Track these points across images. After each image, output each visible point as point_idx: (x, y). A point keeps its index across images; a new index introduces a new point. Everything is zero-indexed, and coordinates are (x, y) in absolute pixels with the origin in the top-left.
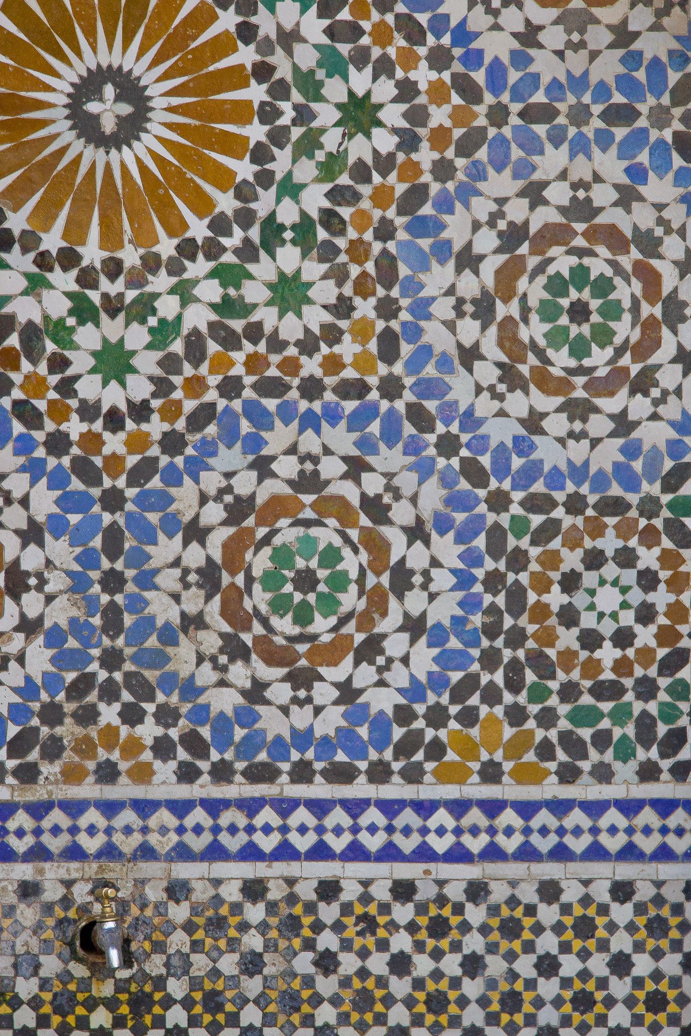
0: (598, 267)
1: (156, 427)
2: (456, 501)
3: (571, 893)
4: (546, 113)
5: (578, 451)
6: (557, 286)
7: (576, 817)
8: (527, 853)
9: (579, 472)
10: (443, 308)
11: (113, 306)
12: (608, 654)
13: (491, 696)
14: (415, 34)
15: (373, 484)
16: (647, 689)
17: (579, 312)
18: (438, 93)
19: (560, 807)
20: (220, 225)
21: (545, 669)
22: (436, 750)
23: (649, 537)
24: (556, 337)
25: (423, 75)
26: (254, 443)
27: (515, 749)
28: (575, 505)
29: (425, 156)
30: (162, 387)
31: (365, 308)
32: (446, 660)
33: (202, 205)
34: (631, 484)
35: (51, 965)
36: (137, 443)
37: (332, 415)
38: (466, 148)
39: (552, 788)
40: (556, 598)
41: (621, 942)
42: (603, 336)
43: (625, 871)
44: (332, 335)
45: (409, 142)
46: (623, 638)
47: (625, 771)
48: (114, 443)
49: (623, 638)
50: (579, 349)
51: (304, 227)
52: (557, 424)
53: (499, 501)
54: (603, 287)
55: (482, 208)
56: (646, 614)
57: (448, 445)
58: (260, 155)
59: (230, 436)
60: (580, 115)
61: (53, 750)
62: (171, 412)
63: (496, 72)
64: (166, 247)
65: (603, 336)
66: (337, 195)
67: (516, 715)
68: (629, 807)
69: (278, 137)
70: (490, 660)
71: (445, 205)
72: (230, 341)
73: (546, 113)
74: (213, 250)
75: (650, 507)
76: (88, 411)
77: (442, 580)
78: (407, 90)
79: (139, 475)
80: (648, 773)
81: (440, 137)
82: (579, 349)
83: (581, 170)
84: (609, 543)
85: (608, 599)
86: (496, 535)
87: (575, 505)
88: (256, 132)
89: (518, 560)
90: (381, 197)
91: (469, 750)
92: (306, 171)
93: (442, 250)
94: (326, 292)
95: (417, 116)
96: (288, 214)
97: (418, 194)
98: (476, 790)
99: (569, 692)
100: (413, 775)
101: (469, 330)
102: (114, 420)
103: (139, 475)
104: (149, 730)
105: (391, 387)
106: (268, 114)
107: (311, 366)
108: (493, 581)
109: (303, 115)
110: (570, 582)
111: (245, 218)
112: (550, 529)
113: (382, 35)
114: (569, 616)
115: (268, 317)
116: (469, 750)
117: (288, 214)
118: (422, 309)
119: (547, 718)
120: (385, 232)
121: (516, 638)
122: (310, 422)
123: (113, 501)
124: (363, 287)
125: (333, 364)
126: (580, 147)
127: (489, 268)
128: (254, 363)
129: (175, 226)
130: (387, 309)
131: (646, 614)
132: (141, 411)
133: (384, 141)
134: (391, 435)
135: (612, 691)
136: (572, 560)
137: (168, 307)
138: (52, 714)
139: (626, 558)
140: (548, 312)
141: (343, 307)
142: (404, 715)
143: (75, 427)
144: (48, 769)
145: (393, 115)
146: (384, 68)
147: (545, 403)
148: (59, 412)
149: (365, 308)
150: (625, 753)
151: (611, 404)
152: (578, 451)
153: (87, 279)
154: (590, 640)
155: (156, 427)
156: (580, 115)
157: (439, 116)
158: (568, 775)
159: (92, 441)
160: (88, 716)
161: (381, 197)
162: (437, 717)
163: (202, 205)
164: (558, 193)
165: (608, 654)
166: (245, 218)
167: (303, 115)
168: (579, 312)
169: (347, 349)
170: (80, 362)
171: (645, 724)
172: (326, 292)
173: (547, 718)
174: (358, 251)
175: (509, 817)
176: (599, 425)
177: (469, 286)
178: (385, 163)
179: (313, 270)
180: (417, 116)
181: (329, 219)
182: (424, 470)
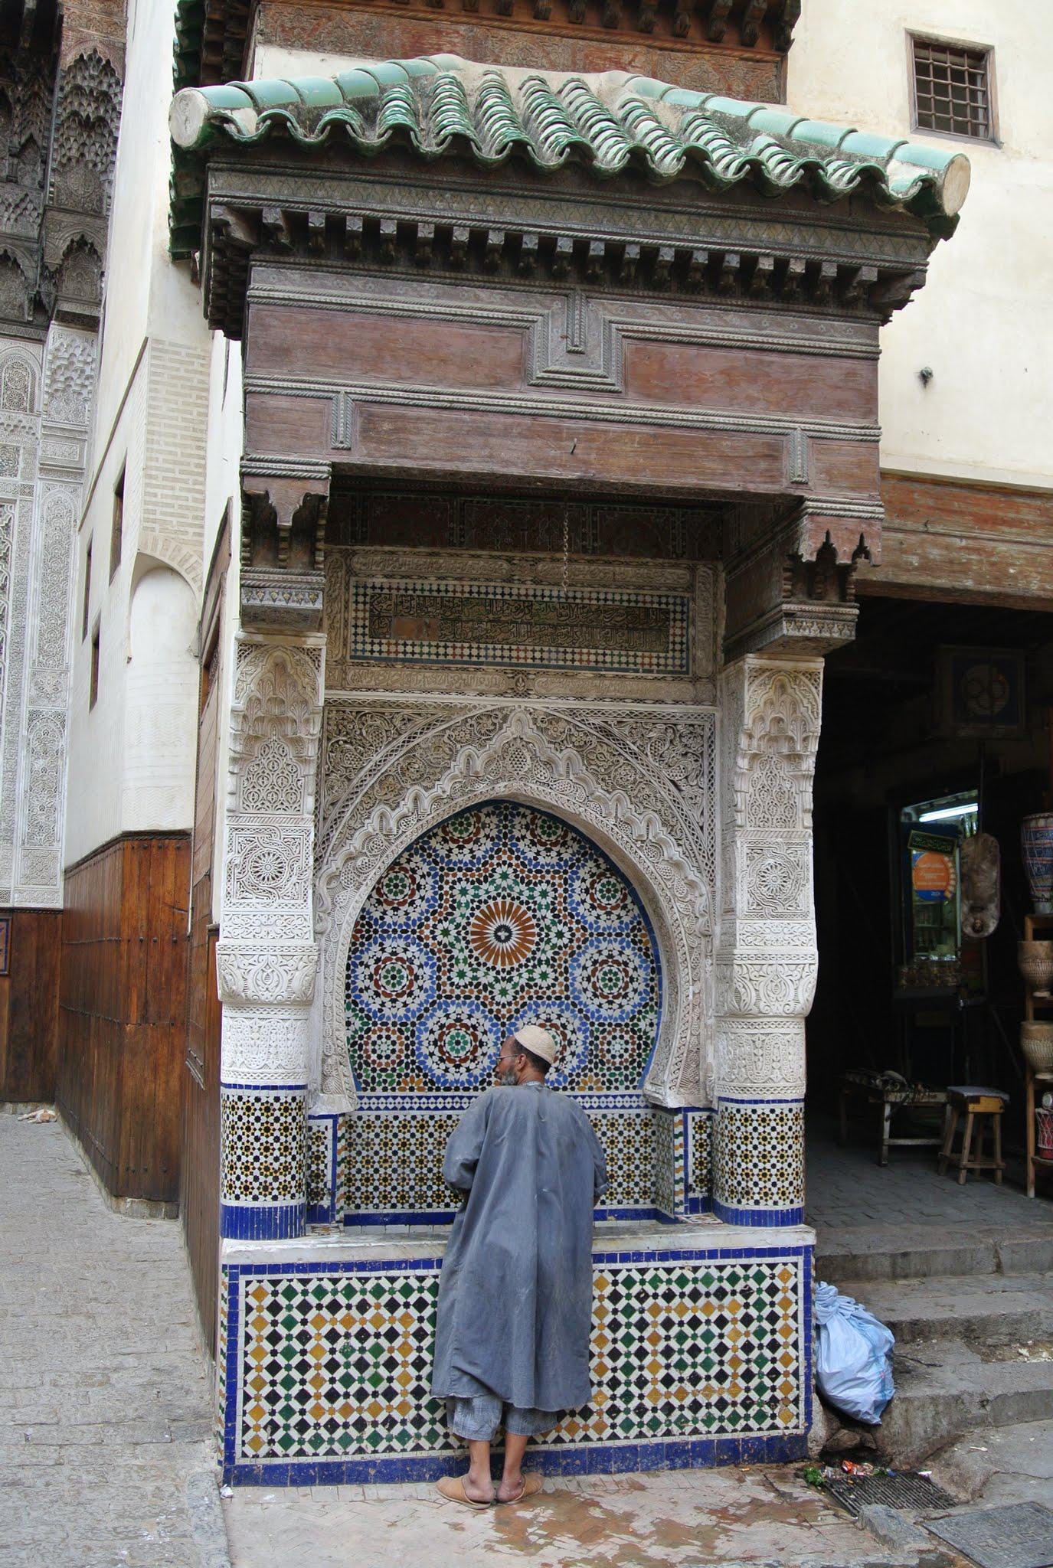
0: (614, 969)
1: (513, 1007)
2: (584, 1024)
3: (609, 1117)
4: (601, 934)
5: (610, 1012)
6: (605, 974)
7: (611, 1099)
8: (599, 1107)
9: (611, 1017)
10: (579, 979)
11: (504, 979)
12: (618, 1060)
13: (591, 1070)
14: (572, 917)
15: (563, 1020)
16: (626, 1068)
17: (610, 980)
18: (578, 930)
19: (607, 1096)
20: (528, 960)
21: (603, 1064)
22: (578, 1083)
23: (627, 1032)
24: (605, 986)
25: (574, 926)
26: (536, 1011)
27: (597, 1082)
28: (610, 1025)
29: (575, 944)
30: (515, 998)
31: (561, 979)
32: (581, 1061)
33: (524, 956)
34: (622, 1019)
36: (509, 1011)
37: (554, 1004)
38: (584, 942)
39: (605, 1092)
40: (606, 1047)
41: (621, 1128)
42: (616, 985)
43: (622, 1111)
44: (554, 985)
45: (571, 941)
46: (621, 1056)
47: (622, 1088)
48: (504, 1011)
49: (621, 1056)
50: (611, 988)
51: (547, 962)
52: (606, 1006)
53: (592, 1024)
54: (616, 974)
55: (588, 956)
56: (626, 1050)
57: (580, 1011)
58: (538, 944)
59: (530, 1009)
60: (610, 935)
61: (489, 1083)
62: (517, 1004)
63: (591, 925)
64: (516, 965)
65: (616, 985)
66: (556, 953)
67: (596, 1075)
68: (623, 1096)
69: (542, 940)
70: (591, 1062)
71: (579, 955)
72: (530, 987)
73: (601, 934)
74: (526, 966)
75: (627, 1025)
76: (498, 1004)
77: (579, 1043)
78: (571, 929)
79: (510, 1018)
80: (627, 1088)
81: (578, 940)
82: (611, 988)
83: (610, 947)
84: (618, 1034)
85: (618, 1047)
86: (592, 1032)
87: (610, 1025)
88: (536, 939)
89: (597, 1038)
90: (565, 953)
91: (585, 1083)
92: (548, 947)
93: (579, 966)
94: (552, 975)
95: (573, 935)
96: (544, 958)
97: (572, 954)
98: (587, 1092)
99: (609, 1069)
100: (573, 1089)
101: (585, 984)
102: (504, 1006)
103: (510, 1018)
105: (567, 998)
106: (539, 935)
107: (549, 993)
108: (591, 1043)
109: (547, 935)
110: (609, 1043)
111: (534, 958)
112: (604, 1031)
113: (565, 917)
114: (609, 1051)
115: (539, 981)
116: (585, 1083)
117: (544, 958)
118: (574, 979)
119: (604, 1075)
120: (566, 961)
121: (596, 1056)
122: (549, 1006)
123: (503, 1024)
124: (561, 974)
125: (554, 992)
126: (610, 942)
127: (590, 969)
128: (536, 992)
129: (518, 960)
130: (566, 979)
131: (626, 1050)
132: (510, 1004)
133: (566, 941)
134: (567, 1009)
136: (609, 1038)
137: (516, 979)
139: (622, 1037)
140: (603, 980)
141: (556, 979)
142: (571, 1075)
143: (495, 1007)
145: (568, 935)
146: (565, 924)
147: (603, 1001)
148: (491, 1004)
149: (561, 979)
150: (622, 1083)
151: (617, 1001)
152: (610, 1012)
153: (498, 973)
154: (614, 1057)
155: (513, 1007)
156: (610, 935)
157: (578, 935)
158: (609, 1088)
159: (499, 1011)
161: (565, 953)
162: (578, 1075)
163: (524, 956)
164: (605, 953)
165: (618, 1060)
166: (534, 958)
167: (547, 935)
168: (610, 980)
169: (557, 988)
170: (496, 992)
171: (626, 1077)
172: (552, 975)
173: (604, 1075)
174: (560, 966)
175: (595, 1099)
176: (615, 1006)
177: (585, 974)
178: (566, 946)
179: (549, 970)
180: (573, 935)
182: (575, 1017)
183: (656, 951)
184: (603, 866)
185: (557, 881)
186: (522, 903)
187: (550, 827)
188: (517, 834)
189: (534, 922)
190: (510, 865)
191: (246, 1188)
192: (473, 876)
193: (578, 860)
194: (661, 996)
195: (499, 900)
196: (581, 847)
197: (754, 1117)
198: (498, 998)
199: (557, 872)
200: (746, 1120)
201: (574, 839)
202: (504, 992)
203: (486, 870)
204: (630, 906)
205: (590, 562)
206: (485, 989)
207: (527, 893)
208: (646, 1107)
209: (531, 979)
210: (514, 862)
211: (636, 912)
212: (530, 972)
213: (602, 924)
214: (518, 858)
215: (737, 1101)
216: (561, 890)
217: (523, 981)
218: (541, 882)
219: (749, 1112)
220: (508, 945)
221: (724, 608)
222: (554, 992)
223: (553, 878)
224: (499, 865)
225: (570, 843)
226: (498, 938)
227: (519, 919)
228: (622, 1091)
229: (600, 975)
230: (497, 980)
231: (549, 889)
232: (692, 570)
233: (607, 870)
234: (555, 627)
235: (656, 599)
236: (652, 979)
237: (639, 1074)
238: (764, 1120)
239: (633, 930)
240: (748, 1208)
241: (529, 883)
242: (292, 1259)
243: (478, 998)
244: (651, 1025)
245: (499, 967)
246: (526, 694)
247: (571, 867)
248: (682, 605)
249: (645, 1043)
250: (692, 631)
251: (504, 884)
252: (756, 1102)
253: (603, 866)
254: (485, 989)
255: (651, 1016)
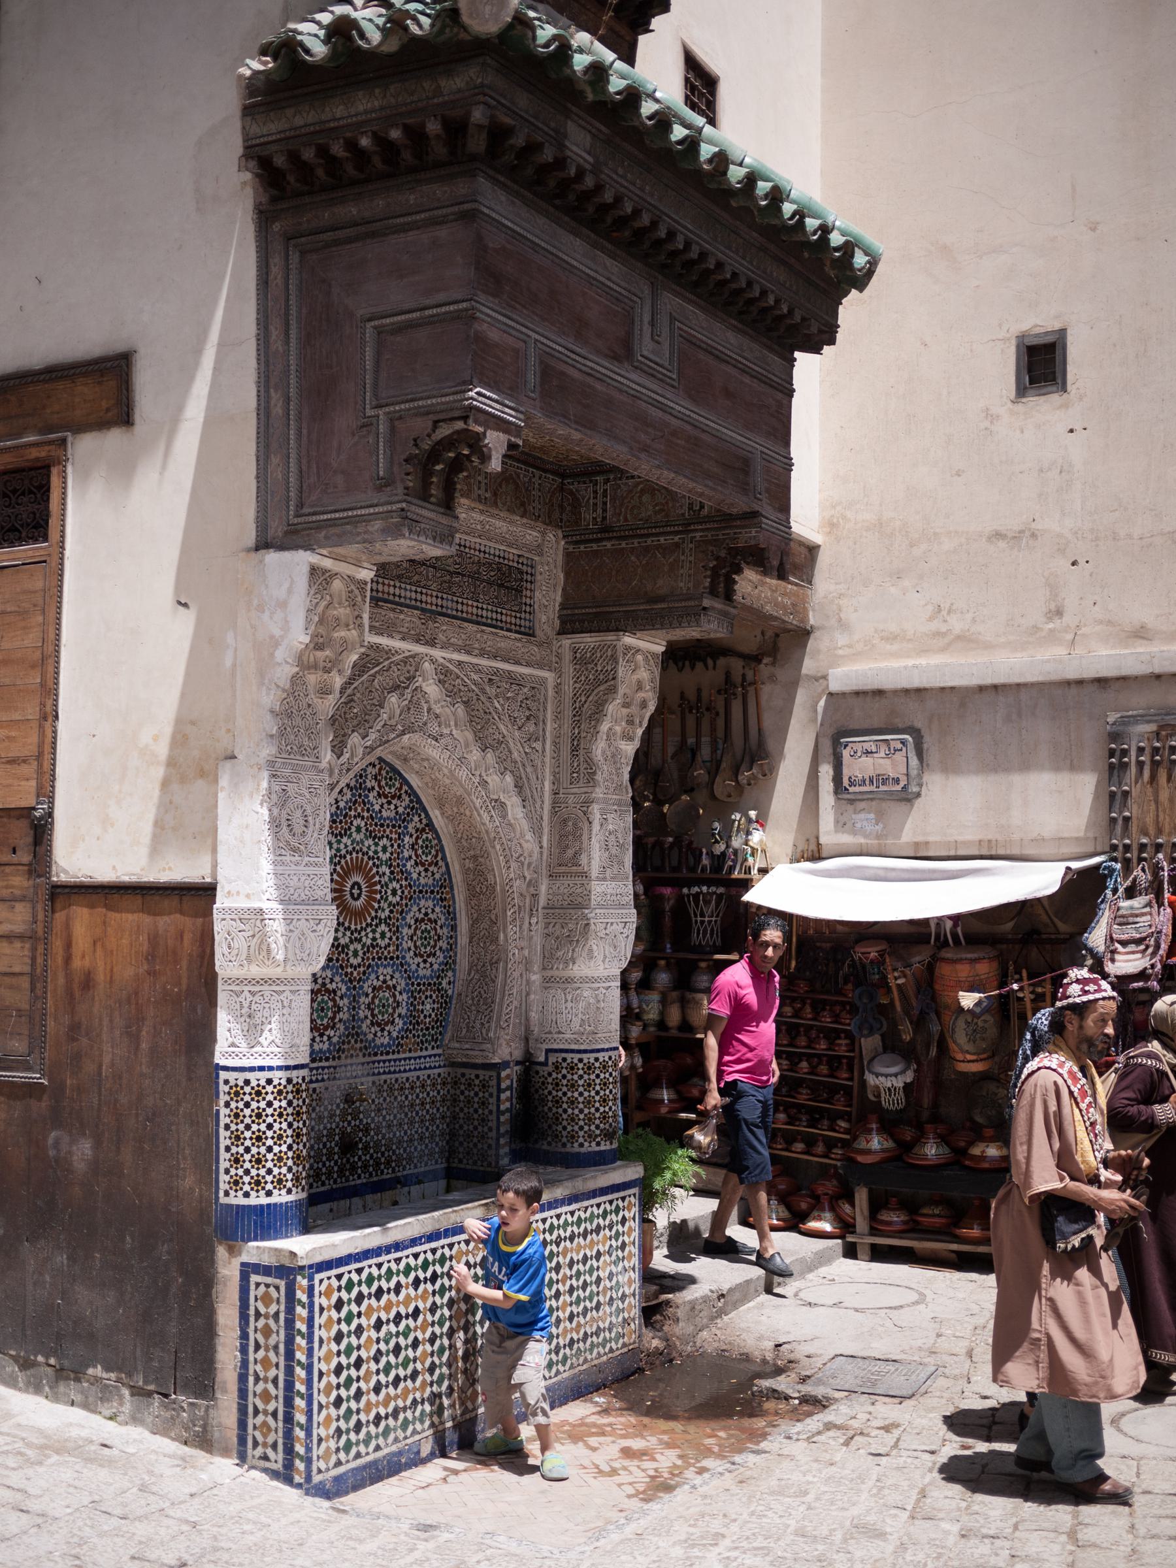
1: (362, 969)
35: (342, 1106)
44: (389, 945)
53: (413, 984)
57: (406, 971)
66: (391, 912)
76: (351, 966)
80: (433, 1048)
84: (428, 993)
91: (407, 1045)
95: (403, 892)
104: (358, 1045)
105: (398, 958)
110: (423, 1003)
115: (379, 941)
123: (354, 988)
130: (397, 939)
135: (427, 1029)
138: (343, 1043)
143: (349, 970)
144: (343, 1056)
149: (394, 938)
155: (362, 969)
160: (349, 1042)
169: (391, 948)
181: (390, 918)
183: (455, 909)
184: (424, 821)
185: (394, 836)
186: (369, 858)
187: (391, 779)
188: (369, 785)
189: (377, 878)
190: (363, 818)
191: (280, 1181)
192: (336, 828)
193: (408, 814)
194: (456, 955)
195: (354, 855)
196: (411, 801)
197: (597, 1065)
198: (352, 960)
199: (394, 826)
200: (589, 1068)
201: (406, 792)
202: (356, 954)
203: (346, 823)
204: (440, 863)
205: (482, 512)
206: (343, 951)
207: (373, 848)
208: (445, 1066)
209: (374, 939)
210: (366, 814)
211: (444, 869)
212: (374, 931)
213: (422, 881)
214: (368, 810)
215: (579, 1052)
216: (396, 846)
217: (369, 942)
218: (383, 836)
219: (592, 1061)
220: (358, 903)
221: (562, 576)
222: (389, 952)
223: (391, 832)
224: (355, 817)
225: (404, 796)
226: (352, 895)
227: (368, 878)
228: (430, 1052)
229: (419, 933)
230: (351, 941)
231: (389, 844)
232: (544, 534)
233: (427, 825)
234: (451, 574)
235: (516, 559)
236: (451, 937)
237: (441, 1033)
238: (604, 1067)
239: (441, 887)
240: (590, 1149)
241: (375, 837)
242: (343, 1252)
243: (338, 960)
244: (449, 983)
245: (353, 927)
246: (431, 643)
247: (404, 821)
248: (532, 567)
249: (446, 1002)
250: (537, 594)
251: (358, 837)
252: (598, 1051)
253: (424, 821)
254: (343, 951)
255: (450, 974)
